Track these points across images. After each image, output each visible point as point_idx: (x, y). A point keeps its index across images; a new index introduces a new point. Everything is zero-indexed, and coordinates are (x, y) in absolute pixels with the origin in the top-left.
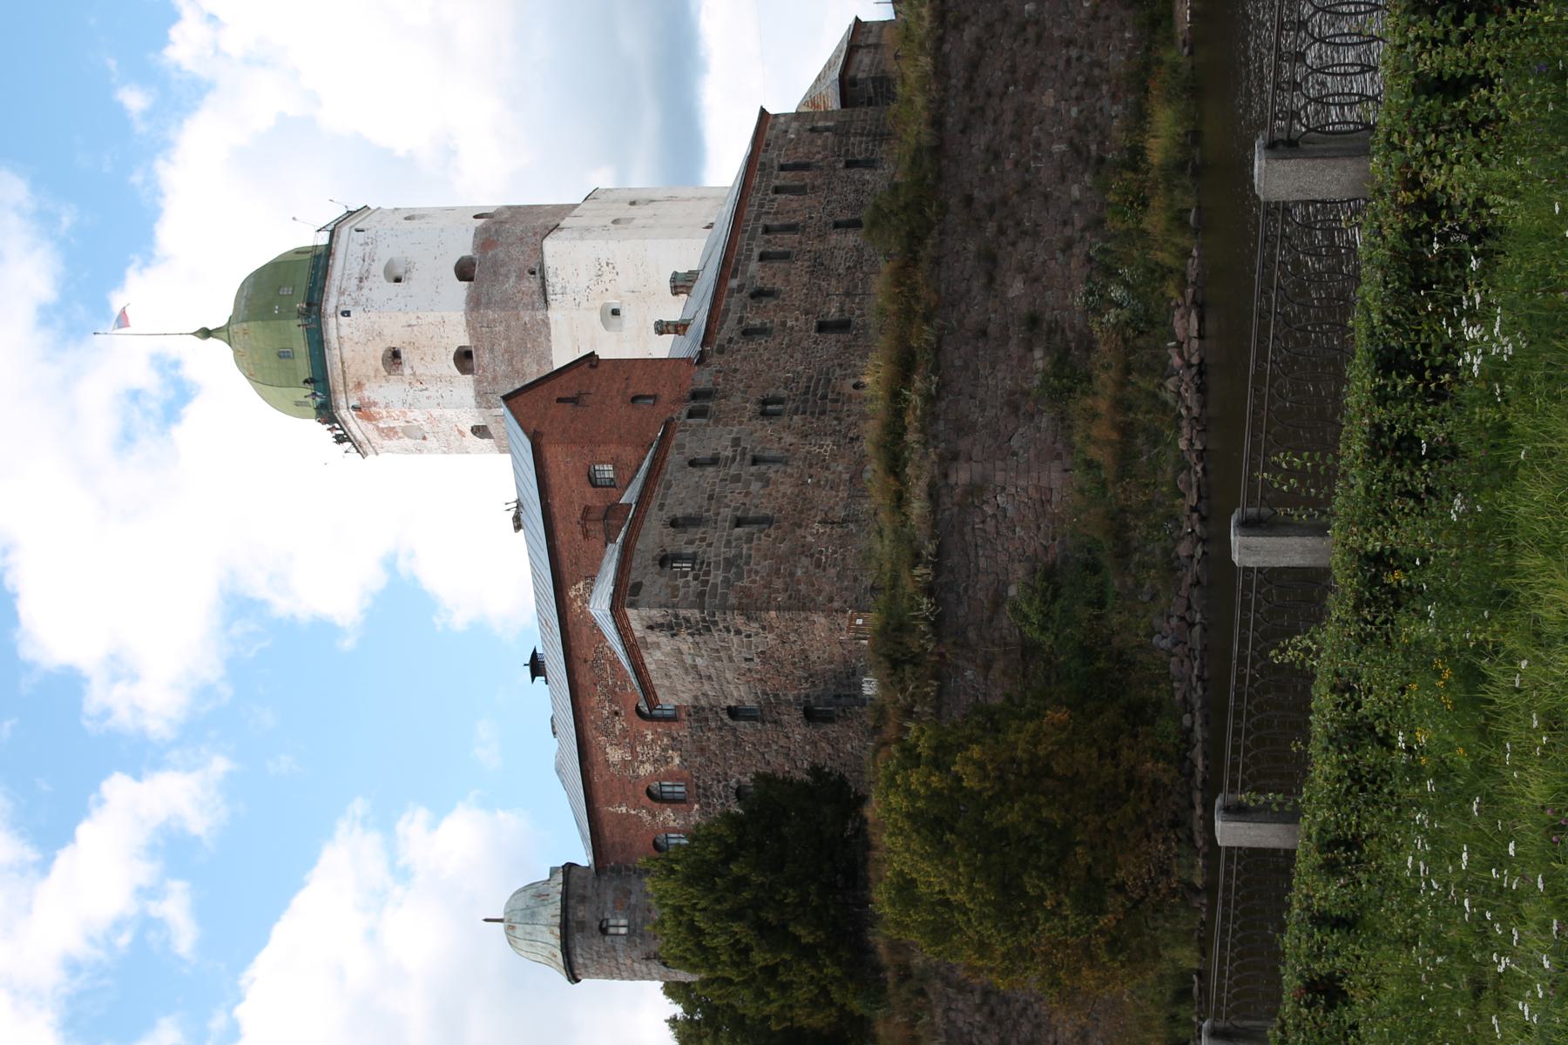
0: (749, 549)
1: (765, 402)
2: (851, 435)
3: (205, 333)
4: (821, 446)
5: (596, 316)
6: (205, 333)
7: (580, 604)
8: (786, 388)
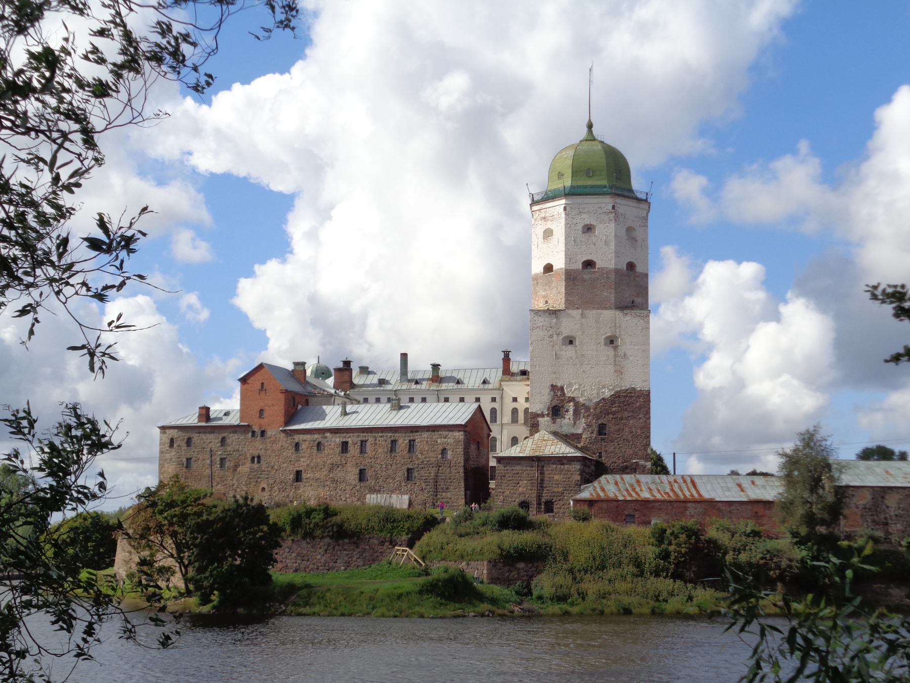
1: (259, 457)
3: (590, 126)
6: (590, 126)
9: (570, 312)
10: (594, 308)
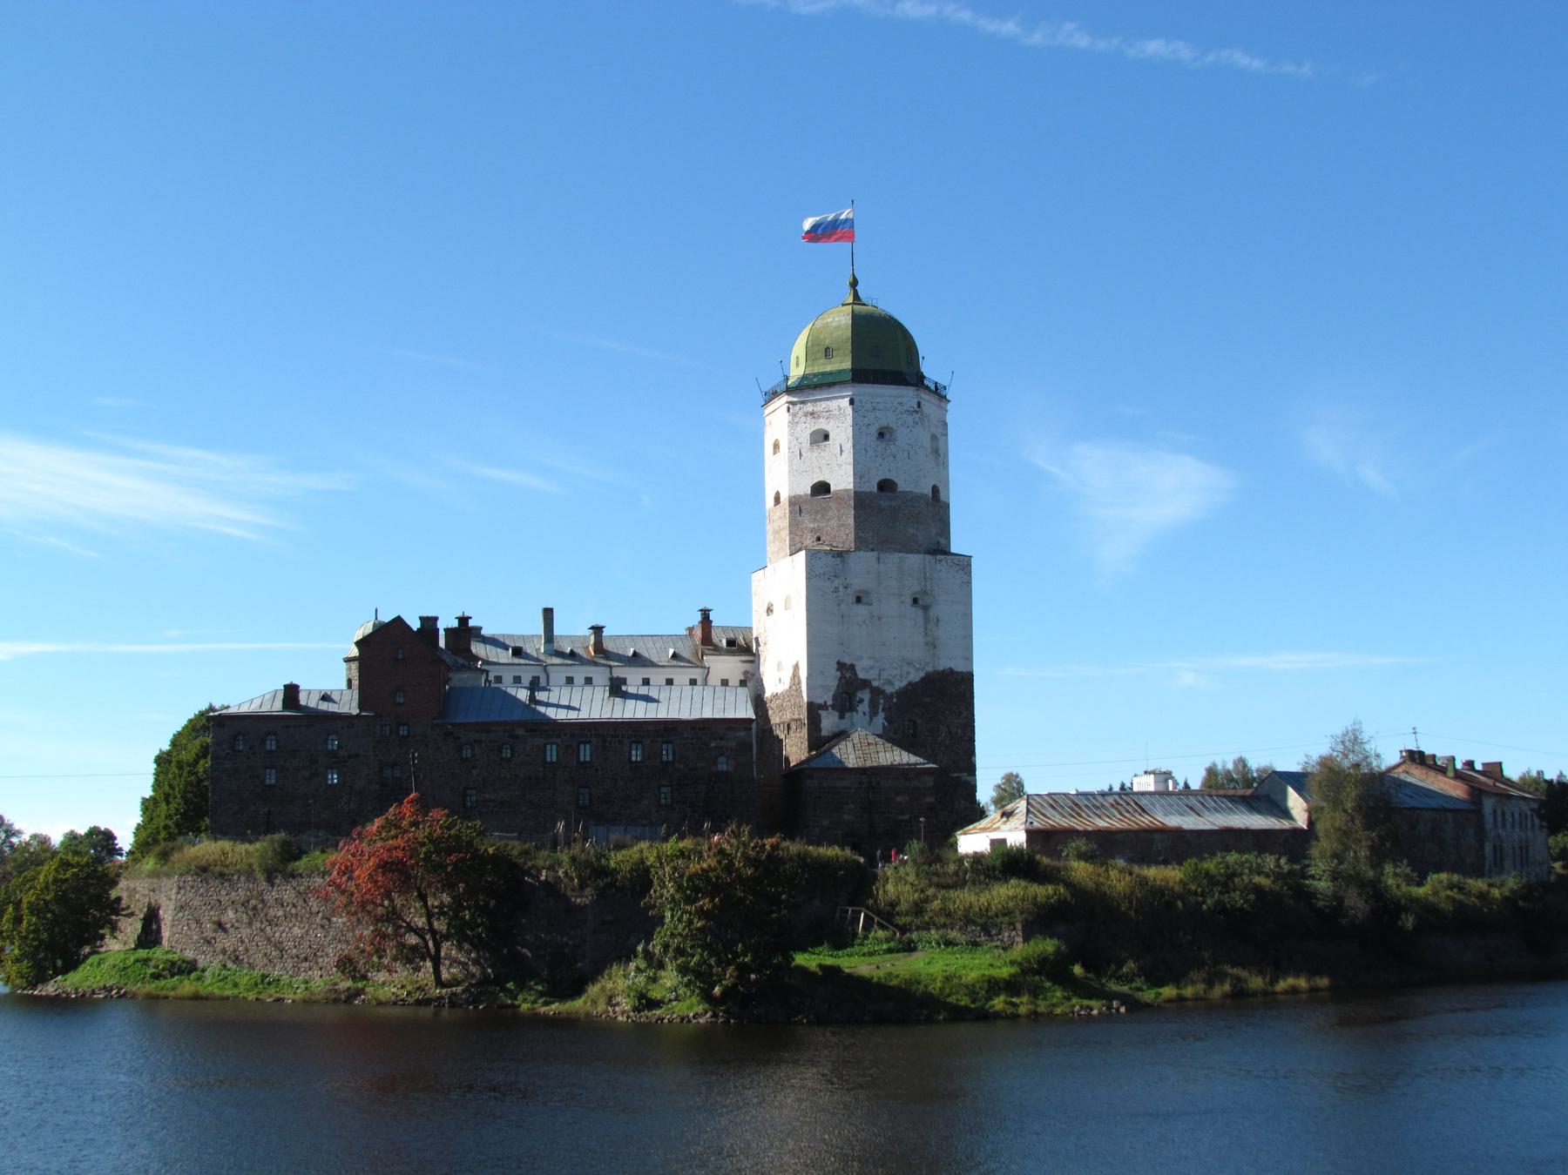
3: (854, 283)
6: (854, 283)
9: (861, 554)
10: (895, 551)
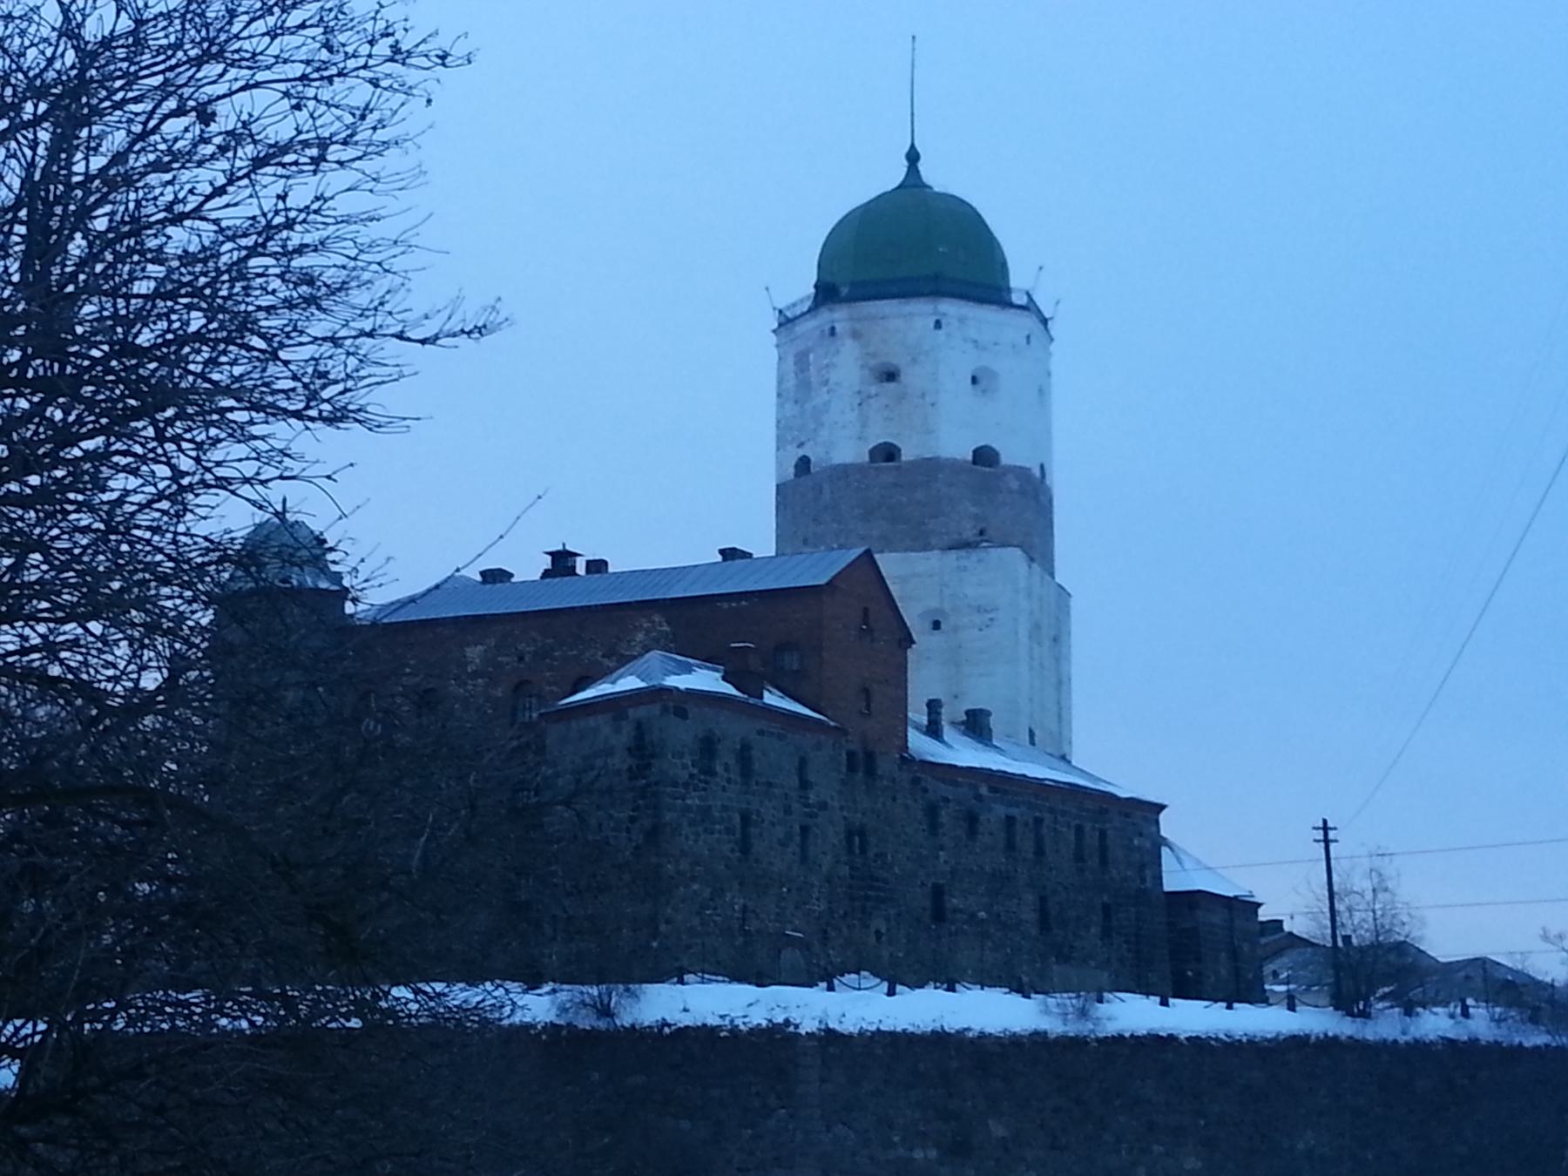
0: (720, 832)
1: (862, 833)
2: (829, 929)
3: (913, 157)
4: (818, 899)
5: (934, 603)
6: (913, 157)
7: (645, 625)
8: (876, 855)
